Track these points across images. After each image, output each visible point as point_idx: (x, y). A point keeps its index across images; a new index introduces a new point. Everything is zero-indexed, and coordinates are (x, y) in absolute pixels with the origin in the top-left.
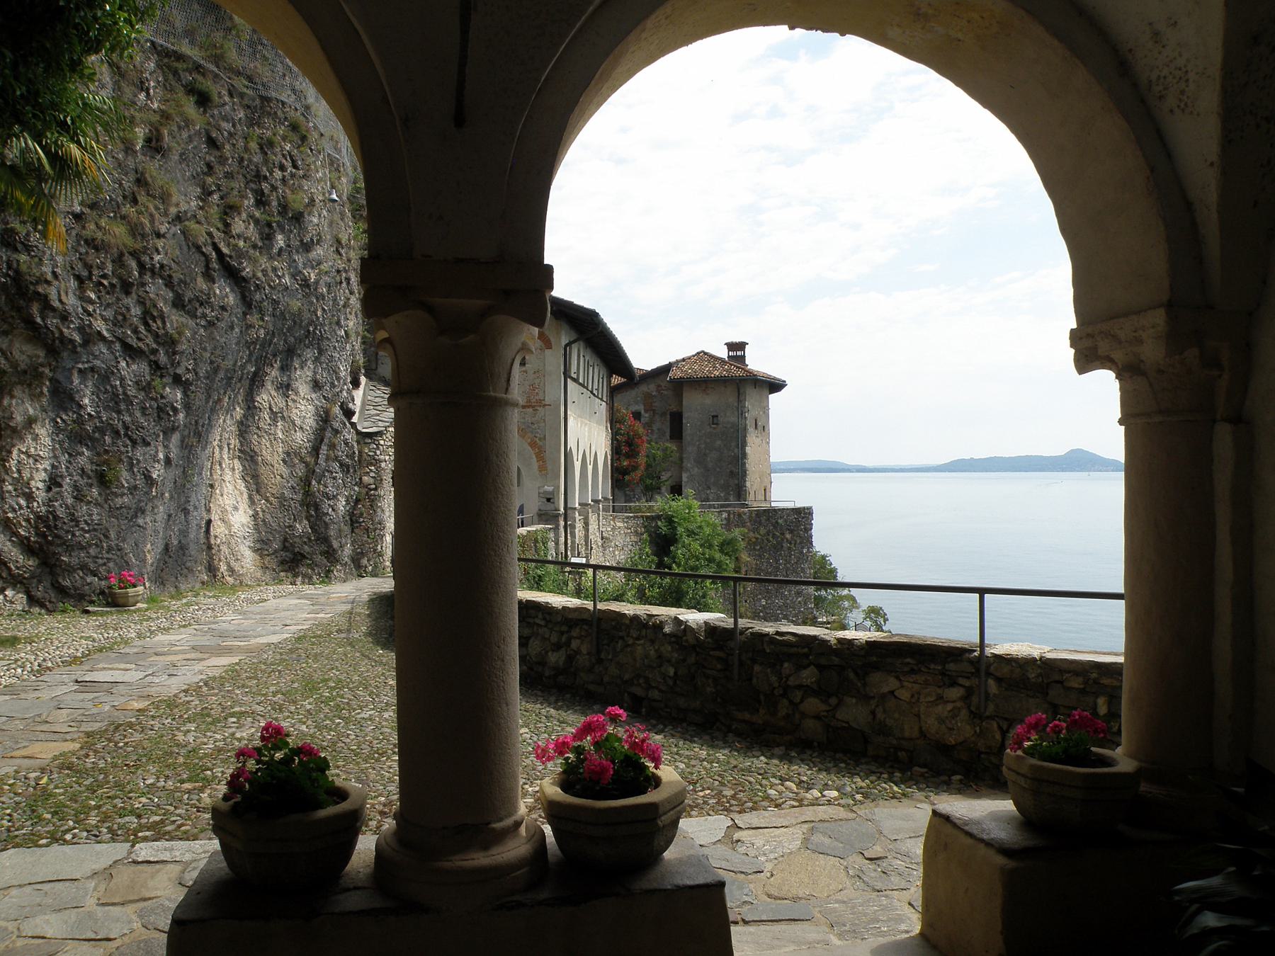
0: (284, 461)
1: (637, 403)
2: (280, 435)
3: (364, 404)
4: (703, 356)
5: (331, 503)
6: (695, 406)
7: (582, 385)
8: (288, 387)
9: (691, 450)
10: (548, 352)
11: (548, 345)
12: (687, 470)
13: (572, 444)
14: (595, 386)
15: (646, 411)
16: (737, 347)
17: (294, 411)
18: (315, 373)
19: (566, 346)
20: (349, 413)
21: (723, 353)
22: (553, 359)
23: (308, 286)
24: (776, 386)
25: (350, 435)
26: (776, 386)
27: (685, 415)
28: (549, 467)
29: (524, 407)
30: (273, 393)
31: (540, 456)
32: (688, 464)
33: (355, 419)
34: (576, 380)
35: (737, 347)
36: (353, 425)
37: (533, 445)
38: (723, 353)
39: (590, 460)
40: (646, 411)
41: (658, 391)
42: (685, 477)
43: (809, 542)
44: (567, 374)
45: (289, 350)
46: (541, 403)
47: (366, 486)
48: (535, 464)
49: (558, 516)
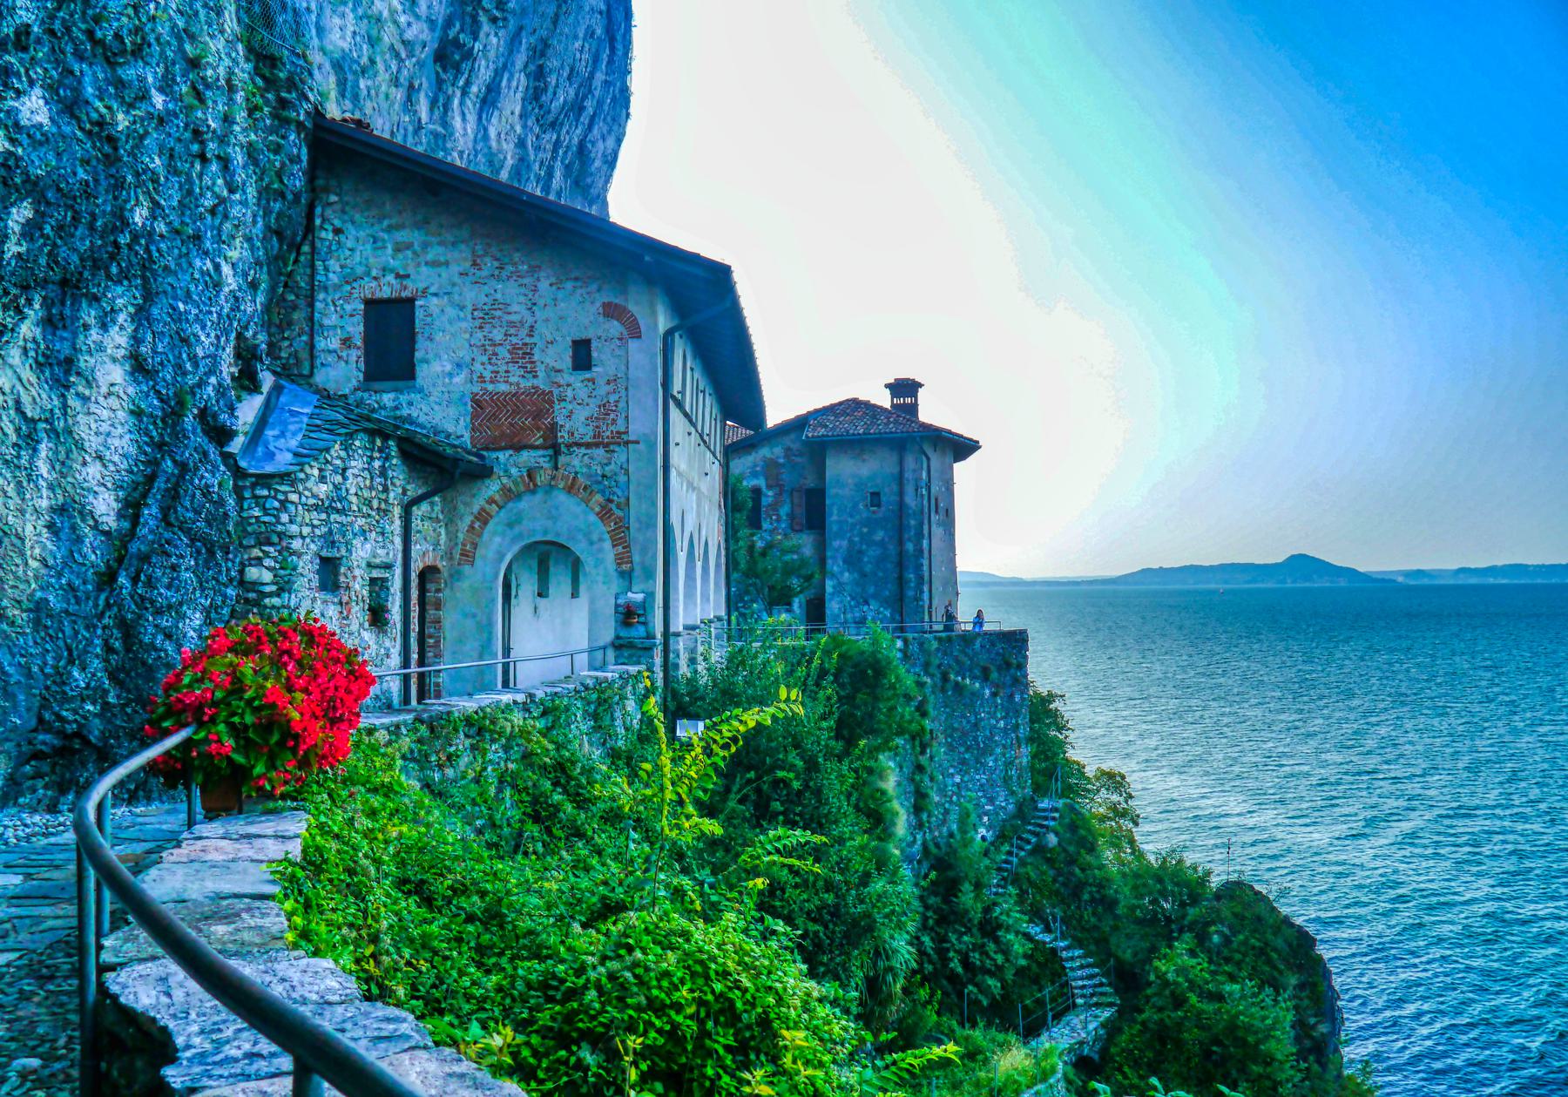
0: (50, 526)
1: (755, 475)
2: (44, 468)
3: (262, 422)
4: (854, 407)
5: (165, 622)
6: (846, 474)
7: (691, 421)
8: (69, 363)
9: (838, 545)
10: (633, 345)
11: (635, 332)
12: (833, 576)
13: (675, 519)
14: (707, 431)
15: (769, 487)
16: (905, 389)
17: (81, 418)
18: (136, 340)
19: (669, 333)
20: (222, 435)
21: (884, 400)
22: (642, 357)
23: (111, 140)
24: (963, 448)
25: (216, 478)
26: (963, 448)
27: (831, 492)
28: (636, 558)
29: (588, 446)
30: (27, 374)
31: (620, 536)
32: (834, 566)
33: (236, 446)
34: (680, 405)
35: (905, 389)
36: (227, 457)
37: (605, 514)
38: (884, 400)
39: (699, 551)
40: (769, 487)
41: (786, 456)
42: (829, 585)
43: (1027, 685)
44: (666, 384)
45: (64, 283)
46: (621, 440)
47: (254, 585)
48: (609, 552)
49: (649, 649)
